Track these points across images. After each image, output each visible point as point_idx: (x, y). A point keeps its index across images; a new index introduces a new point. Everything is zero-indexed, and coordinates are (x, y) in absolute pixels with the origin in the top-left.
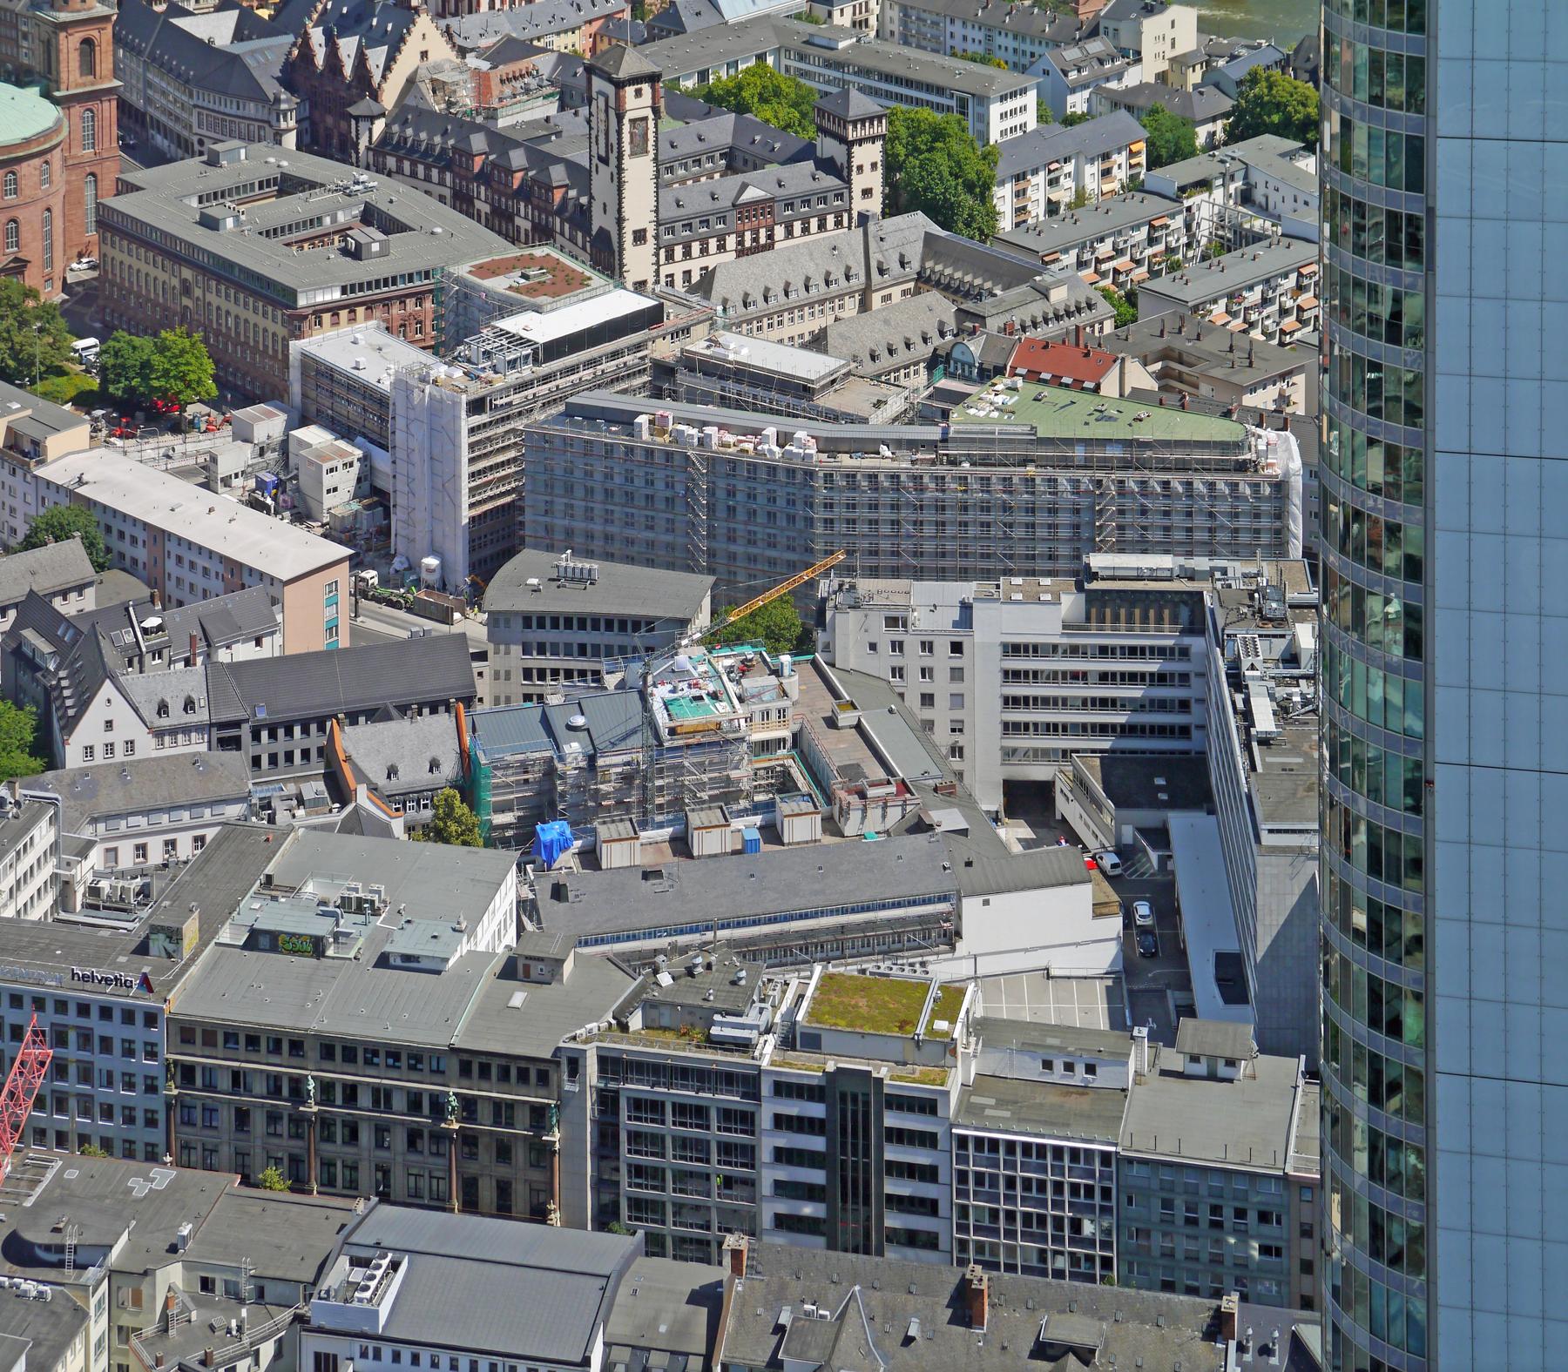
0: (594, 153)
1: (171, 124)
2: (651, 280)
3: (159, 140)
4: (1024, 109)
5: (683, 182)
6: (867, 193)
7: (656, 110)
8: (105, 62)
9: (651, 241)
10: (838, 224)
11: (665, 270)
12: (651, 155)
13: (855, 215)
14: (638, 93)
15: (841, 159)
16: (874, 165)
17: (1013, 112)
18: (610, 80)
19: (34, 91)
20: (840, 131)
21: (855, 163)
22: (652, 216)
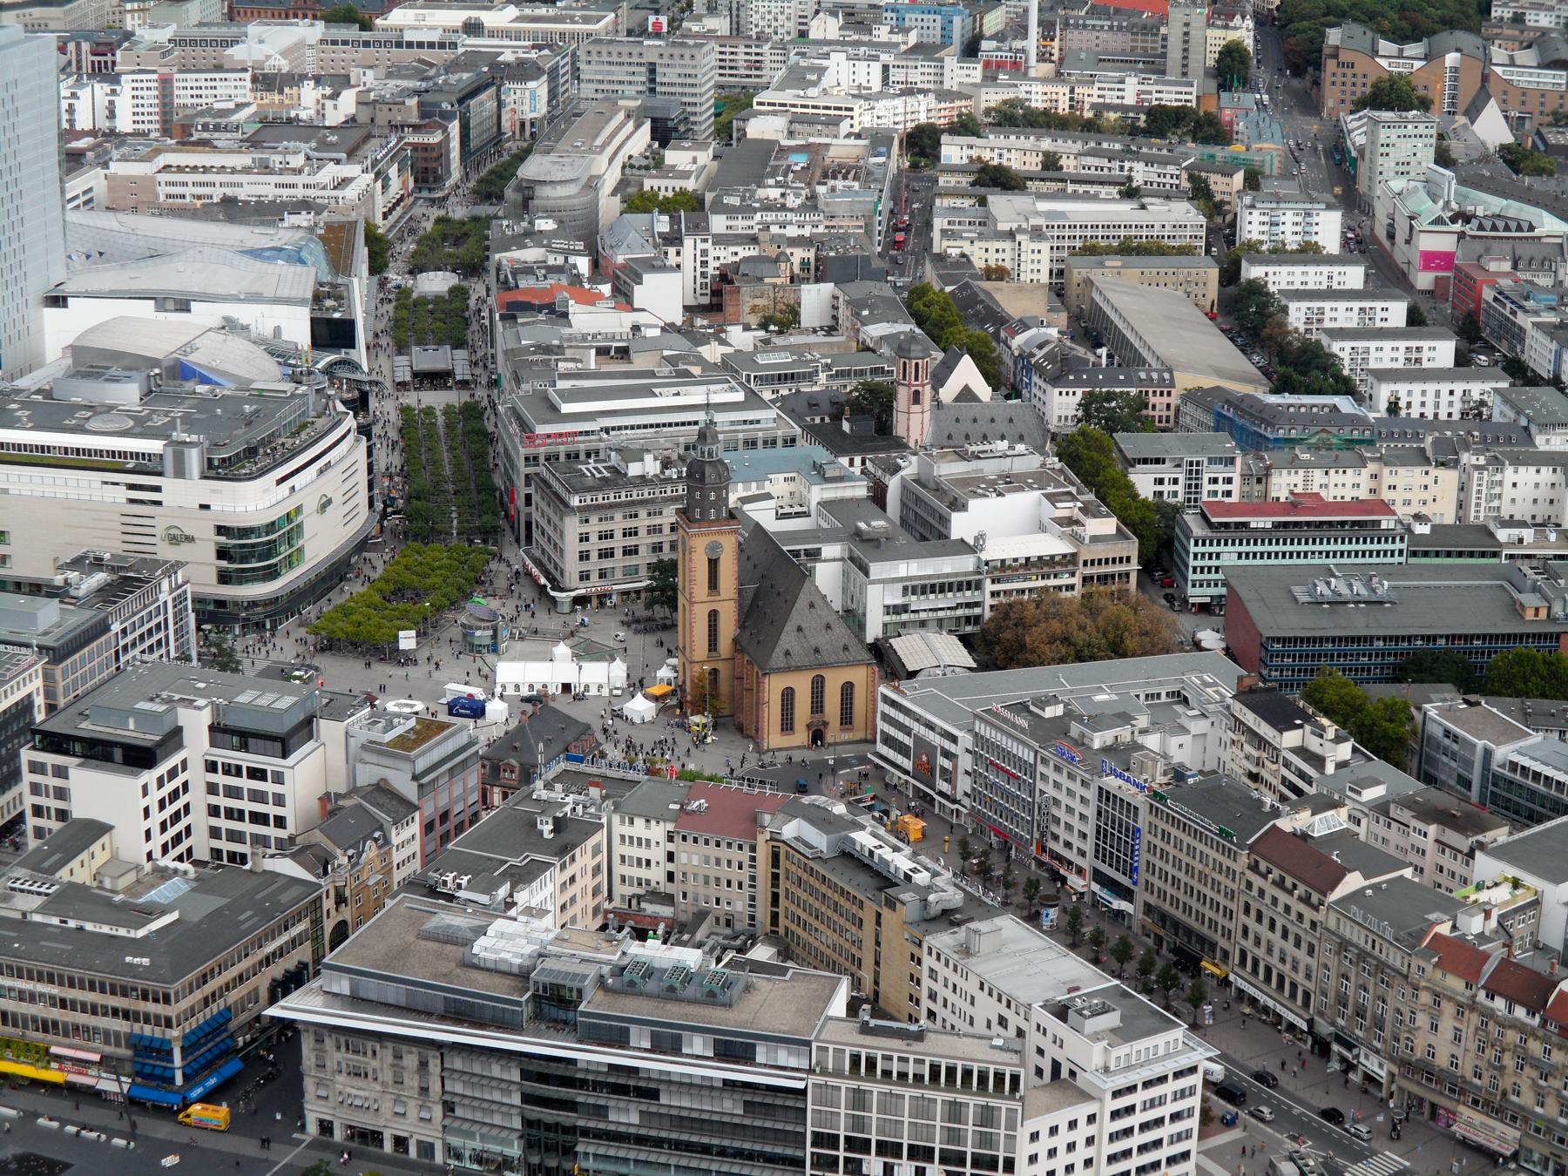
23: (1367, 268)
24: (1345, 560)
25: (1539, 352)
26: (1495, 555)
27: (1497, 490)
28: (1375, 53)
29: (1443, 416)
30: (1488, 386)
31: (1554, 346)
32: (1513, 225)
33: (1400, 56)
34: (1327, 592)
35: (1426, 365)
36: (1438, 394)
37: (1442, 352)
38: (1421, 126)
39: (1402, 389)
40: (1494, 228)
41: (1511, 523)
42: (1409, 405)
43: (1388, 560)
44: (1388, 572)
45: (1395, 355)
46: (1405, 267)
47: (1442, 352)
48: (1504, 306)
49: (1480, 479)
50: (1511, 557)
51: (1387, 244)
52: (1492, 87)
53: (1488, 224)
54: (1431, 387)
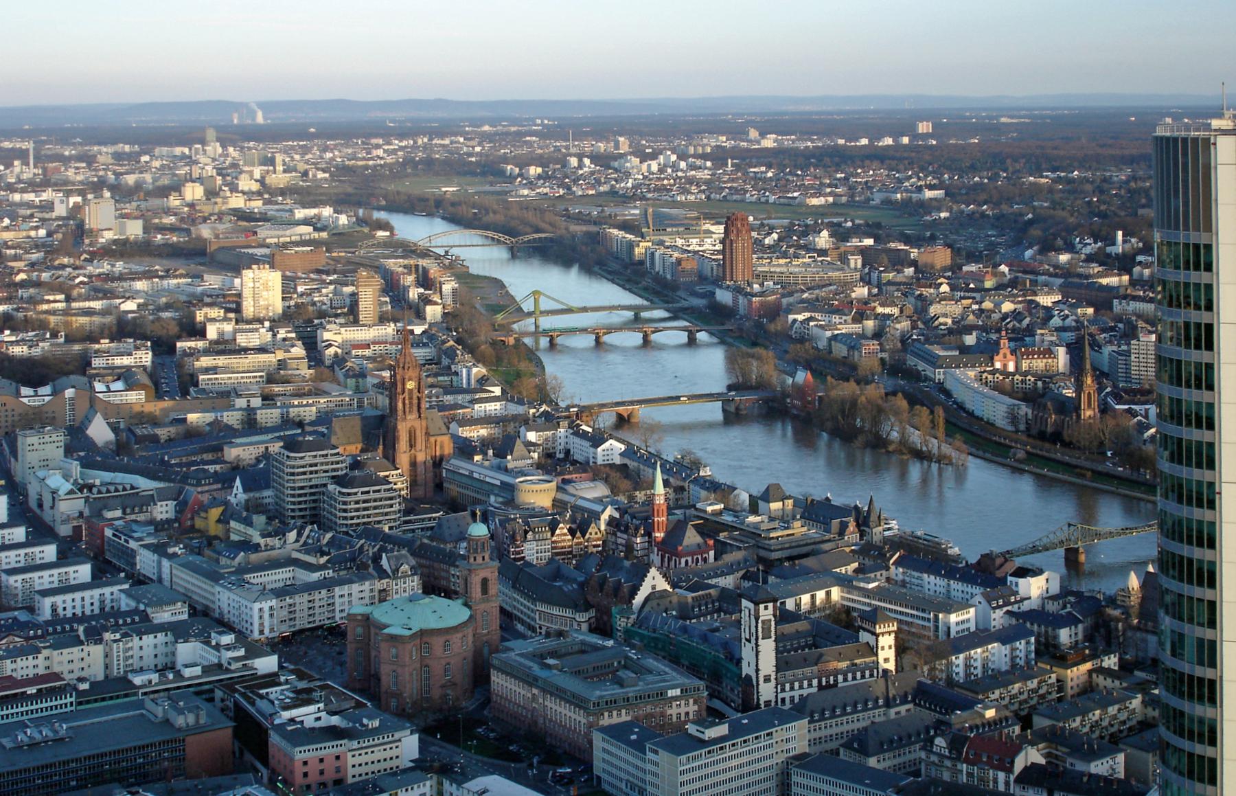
0: (743, 636)
1: (525, 618)
2: (773, 700)
3: (520, 627)
4: (968, 620)
5: (789, 652)
6: (886, 660)
7: (775, 615)
8: (494, 588)
9: (773, 681)
10: (871, 675)
11: (780, 696)
12: (773, 638)
13: (880, 671)
14: (766, 608)
15: (872, 643)
16: (890, 647)
17: (963, 622)
18: (752, 602)
19: (460, 601)
20: (872, 629)
21: (880, 645)
22: (774, 669)
23: (27, 528)
24: (35, 715)
25: (146, 561)
26: (136, 694)
27: (130, 653)
28: (18, 394)
29: (88, 612)
30: (115, 589)
31: (156, 557)
32: (120, 488)
33: (36, 395)
34: (26, 739)
35: (73, 582)
36: (83, 599)
37: (83, 572)
38: (54, 436)
39: (58, 599)
40: (108, 491)
41: (141, 670)
42: (65, 609)
43: (64, 710)
44: (64, 718)
45: (51, 579)
46: (51, 524)
47: (83, 572)
48: (120, 538)
49: (119, 648)
50: (145, 694)
51: (38, 511)
52: (98, 406)
53: (104, 489)
54: (78, 595)
